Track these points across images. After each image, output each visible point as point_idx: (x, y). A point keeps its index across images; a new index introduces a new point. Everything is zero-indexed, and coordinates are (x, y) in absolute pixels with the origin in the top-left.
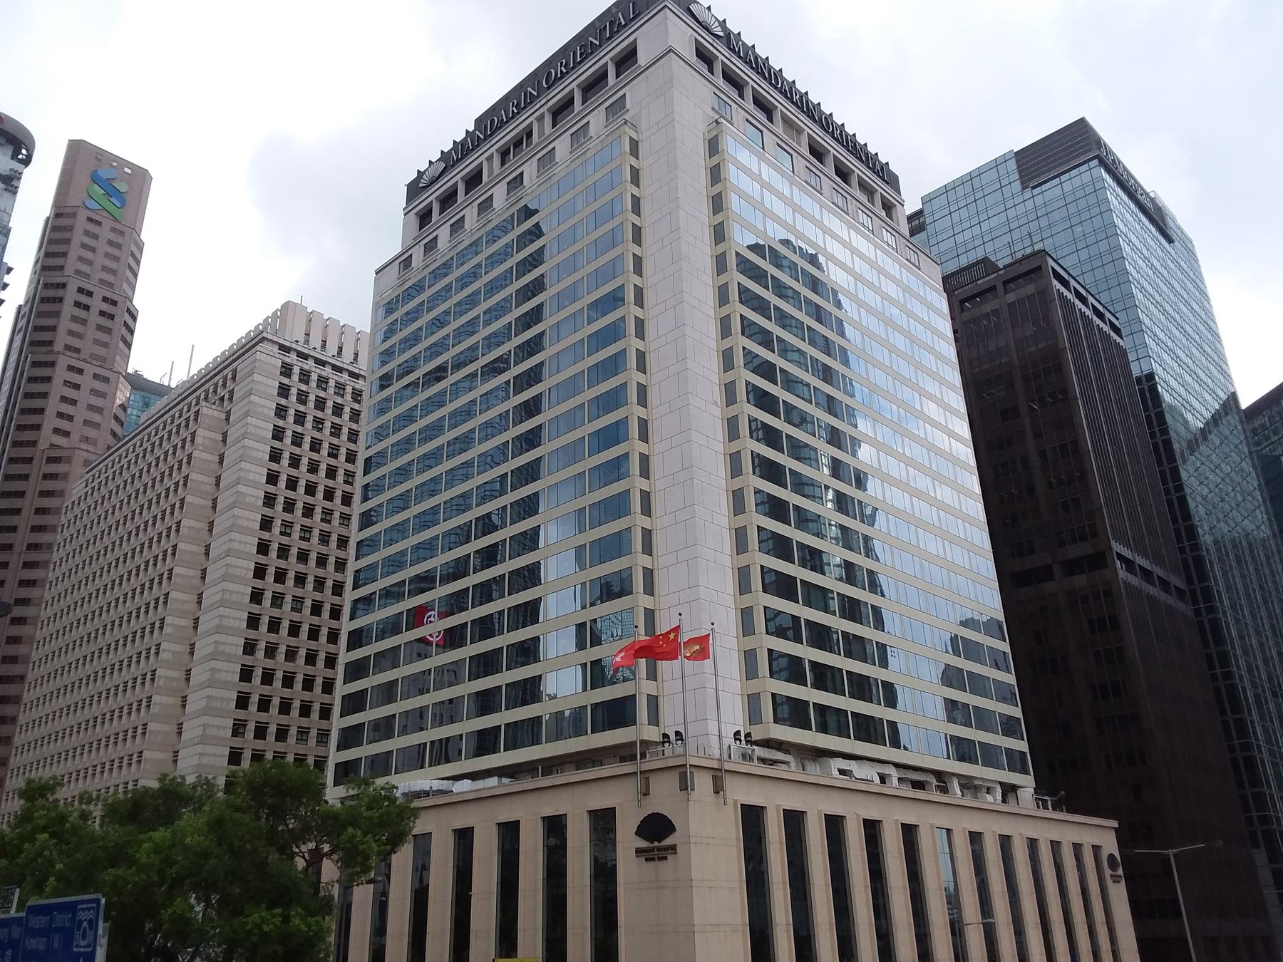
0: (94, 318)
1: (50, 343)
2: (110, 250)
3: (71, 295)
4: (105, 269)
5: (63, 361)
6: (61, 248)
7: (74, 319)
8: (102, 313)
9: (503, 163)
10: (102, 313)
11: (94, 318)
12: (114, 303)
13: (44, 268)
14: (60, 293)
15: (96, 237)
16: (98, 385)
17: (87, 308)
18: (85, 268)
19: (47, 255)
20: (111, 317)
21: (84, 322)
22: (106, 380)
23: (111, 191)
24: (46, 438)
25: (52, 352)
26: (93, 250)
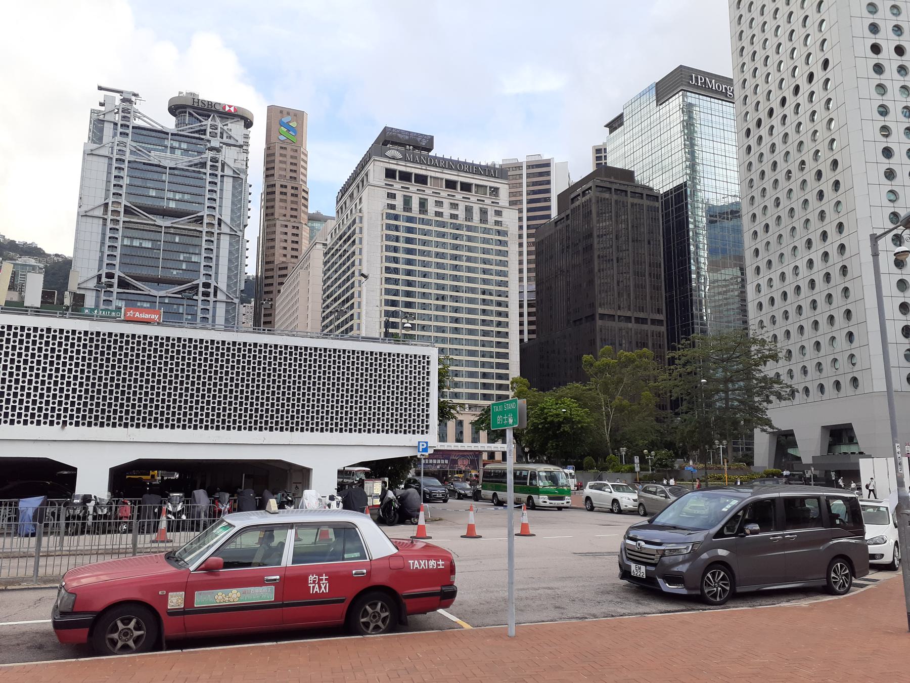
0: (289, 198)
1: (273, 214)
3: (278, 189)
5: (278, 223)
6: (271, 165)
7: (281, 200)
10: (292, 195)
12: (297, 188)
13: (267, 176)
15: (285, 156)
16: (295, 231)
17: (285, 194)
19: (267, 169)
20: (296, 196)
21: (285, 201)
22: (298, 228)
23: (289, 129)
24: (278, 259)
25: (274, 219)
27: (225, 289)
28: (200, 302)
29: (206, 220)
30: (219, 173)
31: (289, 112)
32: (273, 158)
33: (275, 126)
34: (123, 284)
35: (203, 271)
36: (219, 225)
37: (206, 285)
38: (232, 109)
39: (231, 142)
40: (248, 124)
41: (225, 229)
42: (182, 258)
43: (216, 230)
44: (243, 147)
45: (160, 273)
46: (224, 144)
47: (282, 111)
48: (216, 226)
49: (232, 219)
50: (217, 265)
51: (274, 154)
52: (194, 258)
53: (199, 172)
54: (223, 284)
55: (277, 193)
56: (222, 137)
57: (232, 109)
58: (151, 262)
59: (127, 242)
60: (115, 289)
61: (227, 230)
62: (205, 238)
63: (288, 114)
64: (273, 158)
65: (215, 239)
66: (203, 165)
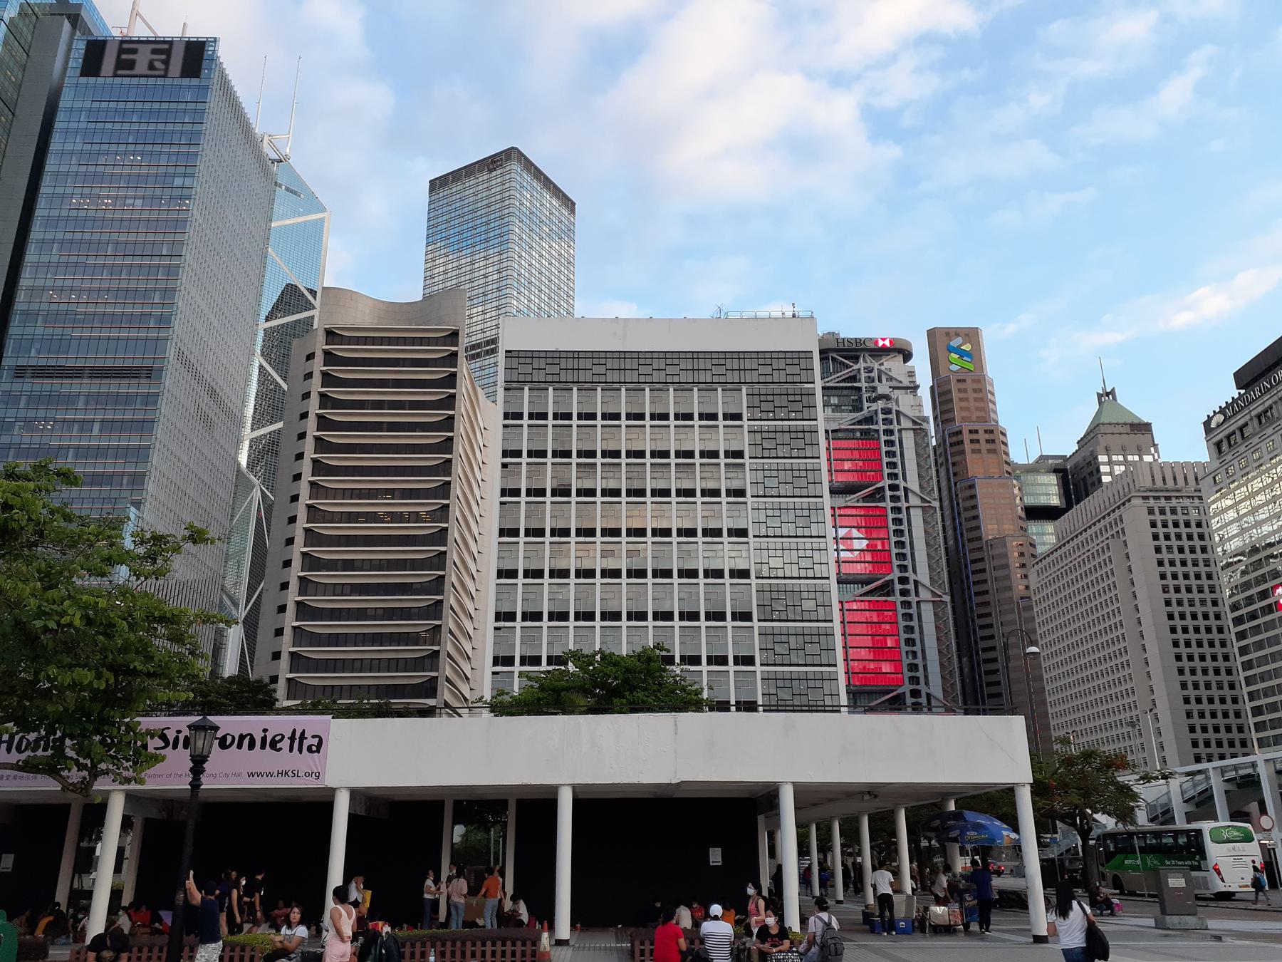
0: (984, 446)
2: (976, 395)
3: (966, 437)
4: (977, 409)
7: (974, 451)
8: (987, 441)
9: (1260, 422)
10: (987, 441)
12: (992, 432)
13: (944, 422)
14: (960, 438)
17: (978, 441)
18: (964, 414)
21: (979, 451)
23: (962, 354)
26: (967, 400)
27: (927, 581)
28: (899, 605)
29: (888, 493)
30: (895, 427)
31: (957, 332)
32: (948, 397)
33: (942, 354)
35: (896, 562)
37: (903, 580)
38: (887, 343)
39: (894, 384)
40: (907, 356)
41: (914, 500)
43: (903, 504)
44: (915, 388)
46: (894, 388)
47: (950, 333)
48: (903, 498)
49: (920, 486)
51: (950, 391)
53: (868, 431)
54: (923, 575)
55: (967, 442)
56: (880, 381)
57: (887, 343)
62: (891, 516)
63: (957, 335)
64: (948, 397)
65: (903, 516)
66: (869, 420)
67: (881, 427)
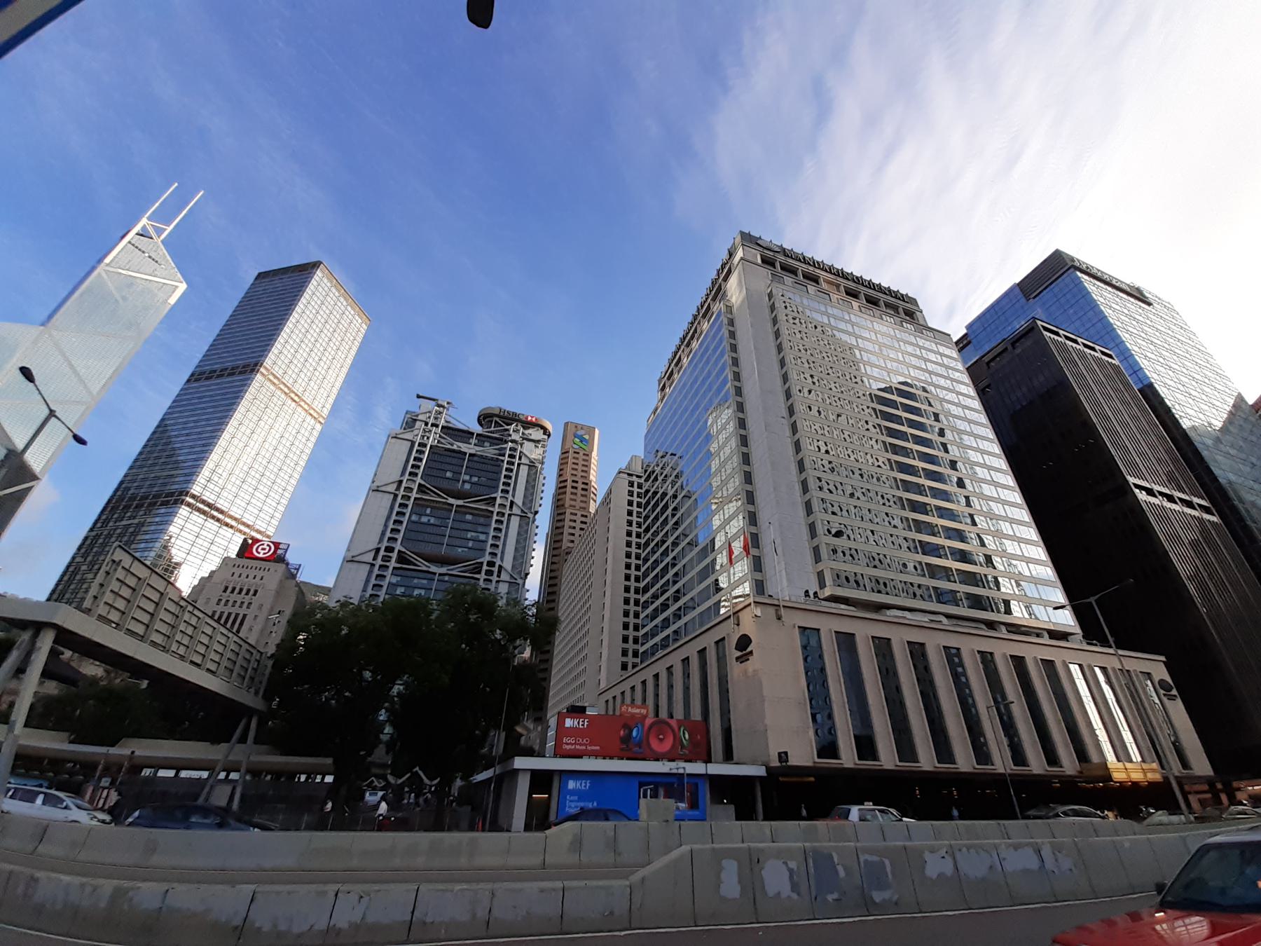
0: (580, 492)
3: (569, 484)
5: (568, 511)
11: (580, 492)
16: (584, 519)
24: (566, 544)
29: (499, 501)
34: (402, 558)
35: (489, 550)
36: (511, 507)
37: (491, 564)
41: (516, 510)
42: (469, 535)
43: (507, 512)
45: (444, 550)
50: (504, 545)
52: (482, 537)
54: (508, 564)
58: (438, 539)
59: (414, 518)
60: (393, 564)
61: (519, 512)
62: (495, 517)
67: (506, 459)
